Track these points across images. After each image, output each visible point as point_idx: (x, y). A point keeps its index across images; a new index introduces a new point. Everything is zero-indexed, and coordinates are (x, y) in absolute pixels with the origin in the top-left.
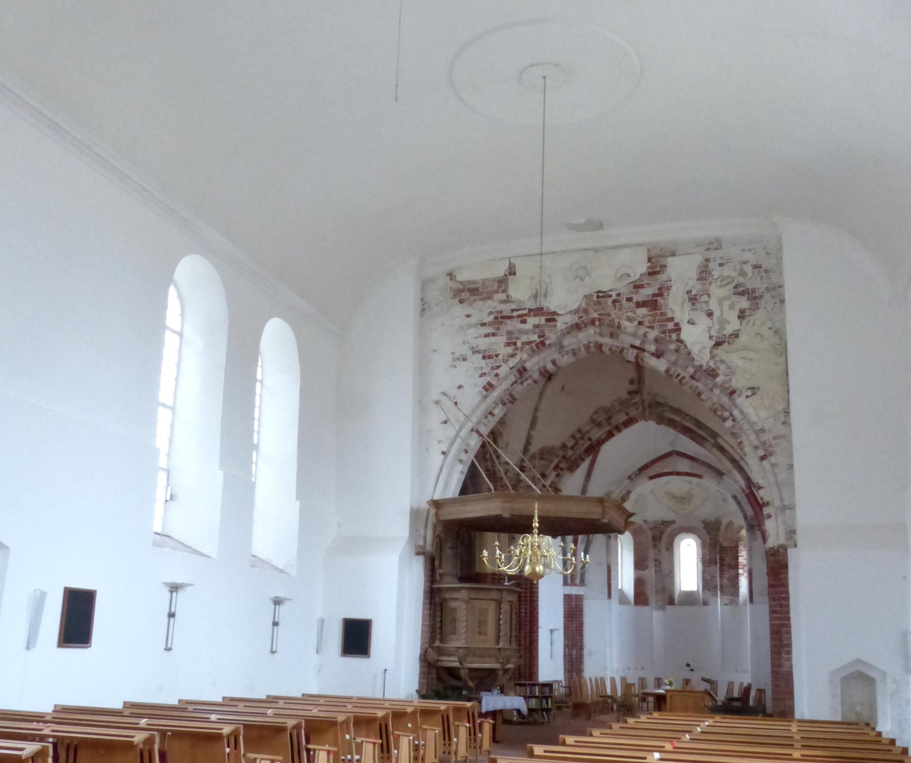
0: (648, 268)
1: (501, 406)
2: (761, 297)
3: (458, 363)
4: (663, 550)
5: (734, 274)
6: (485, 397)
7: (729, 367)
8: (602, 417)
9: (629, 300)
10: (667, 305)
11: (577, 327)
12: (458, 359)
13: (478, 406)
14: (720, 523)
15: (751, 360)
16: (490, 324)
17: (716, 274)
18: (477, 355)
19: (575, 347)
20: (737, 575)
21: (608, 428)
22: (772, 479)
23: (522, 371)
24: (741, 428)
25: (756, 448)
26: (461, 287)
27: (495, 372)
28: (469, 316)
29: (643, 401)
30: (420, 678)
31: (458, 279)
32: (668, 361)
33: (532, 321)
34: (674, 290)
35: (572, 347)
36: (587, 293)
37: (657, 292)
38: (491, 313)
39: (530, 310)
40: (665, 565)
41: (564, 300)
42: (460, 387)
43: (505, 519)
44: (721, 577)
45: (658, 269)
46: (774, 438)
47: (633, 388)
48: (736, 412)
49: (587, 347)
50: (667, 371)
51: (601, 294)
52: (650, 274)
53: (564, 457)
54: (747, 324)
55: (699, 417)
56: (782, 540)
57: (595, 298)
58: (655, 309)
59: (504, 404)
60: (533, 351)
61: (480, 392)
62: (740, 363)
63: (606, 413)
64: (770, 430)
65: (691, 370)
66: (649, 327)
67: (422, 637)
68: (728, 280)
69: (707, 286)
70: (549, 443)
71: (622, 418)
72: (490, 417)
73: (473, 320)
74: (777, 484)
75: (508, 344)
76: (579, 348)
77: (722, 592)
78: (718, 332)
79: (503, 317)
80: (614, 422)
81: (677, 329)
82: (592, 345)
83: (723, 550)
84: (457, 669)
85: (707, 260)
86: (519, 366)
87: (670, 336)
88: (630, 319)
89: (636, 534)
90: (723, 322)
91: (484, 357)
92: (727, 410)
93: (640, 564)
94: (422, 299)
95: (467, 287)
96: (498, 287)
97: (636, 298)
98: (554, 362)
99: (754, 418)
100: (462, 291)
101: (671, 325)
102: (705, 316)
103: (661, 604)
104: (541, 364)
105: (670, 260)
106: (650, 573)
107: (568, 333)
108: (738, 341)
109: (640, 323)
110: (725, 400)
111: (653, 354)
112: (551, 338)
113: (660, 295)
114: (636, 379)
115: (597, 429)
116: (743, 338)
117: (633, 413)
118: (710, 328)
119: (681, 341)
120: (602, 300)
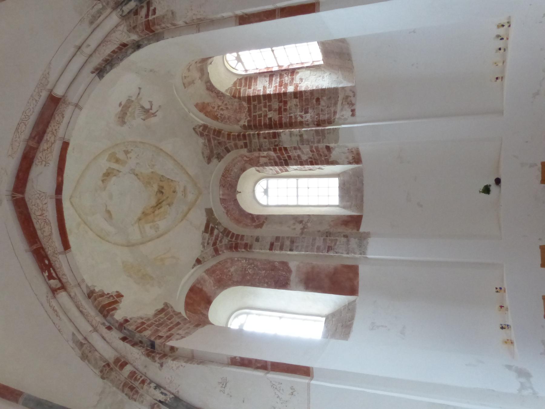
4: (258, 232)
14: (205, 127)
20: (297, 95)
40: (285, 231)
44: (301, 124)
77: (330, 122)
83: (255, 125)
89: (224, 281)
93: (279, 279)
103: (354, 242)
106: (296, 260)
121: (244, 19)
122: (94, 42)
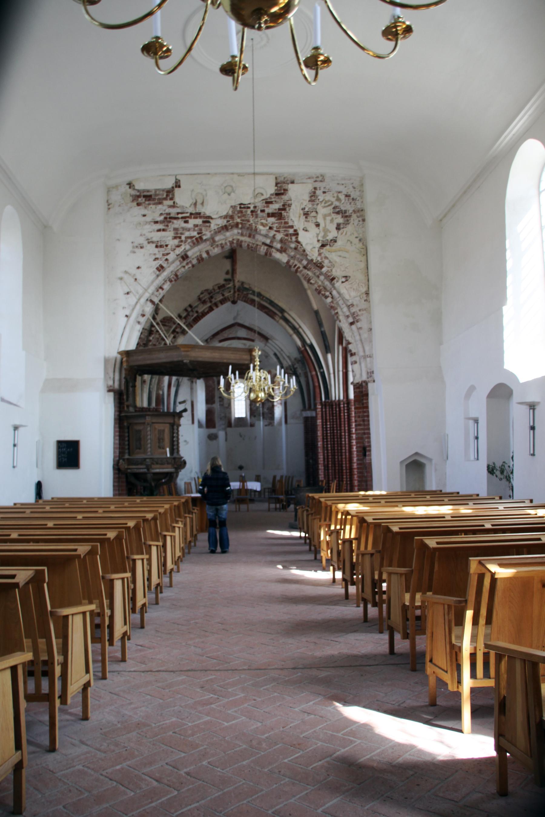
0: (276, 190)
1: (168, 283)
2: (350, 216)
3: (136, 250)
5: (333, 200)
6: (158, 276)
7: (330, 262)
8: (206, 297)
9: (263, 211)
10: (288, 217)
11: (225, 228)
12: (137, 247)
13: (153, 282)
15: (345, 257)
16: (161, 222)
17: (321, 198)
18: (151, 244)
19: (223, 242)
20: (273, 406)
21: (209, 304)
22: (358, 338)
23: (184, 257)
24: (337, 303)
25: (348, 317)
26: (138, 194)
27: (166, 257)
28: (144, 216)
29: (235, 287)
30: (114, 482)
31: (137, 187)
32: (289, 256)
33: (192, 222)
34: (293, 207)
35: (220, 242)
36: (233, 204)
37: (281, 207)
38: (161, 214)
39: (191, 214)
41: (217, 208)
42: (138, 268)
43: (185, 364)
45: (282, 192)
46: (360, 310)
47: (229, 277)
48: (334, 293)
49: (231, 243)
50: (288, 262)
51: (242, 206)
52: (277, 194)
54: (342, 234)
55: (273, 299)
56: (364, 378)
57: (238, 209)
58: (280, 219)
59: (171, 281)
60: (194, 244)
61: (154, 272)
62: (337, 259)
63: (209, 294)
64: (357, 305)
65: (305, 262)
66: (276, 231)
67: (114, 452)
68: (330, 203)
69: (315, 206)
71: (219, 297)
72: (160, 290)
73: (148, 219)
74: (361, 340)
75: (175, 238)
76: (226, 243)
77: (263, 418)
78: (324, 237)
79: (170, 218)
80: (214, 301)
81: (296, 234)
82: (235, 242)
84: (145, 474)
85: (315, 188)
86: (183, 254)
87: (291, 239)
88: (262, 224)
90: (326, 231)
91: (157, 247)
92: (328, 291)
94: (107, 201)
95: (142, 194)
96: (167, 196)
97: (267, 210)
98: (207, 252)
99: (347, 297)
100: (139, 196)
101: (291, 231)
102: (315, 226)
104: (198, 254)
105: (290, 186)
107: (219, 232)
108: (336, 244)
109: (271, 228)
110: (327, 283)
111: (277, 250)
112: (207, 235)
113: (284, 209)
114: (230, 271)
115: (202, 305)
116: (339, 243)
118: (318, 235)
119: (298, 242)
120: (244, 210)
121: (285, 404)
122: (284, 355)
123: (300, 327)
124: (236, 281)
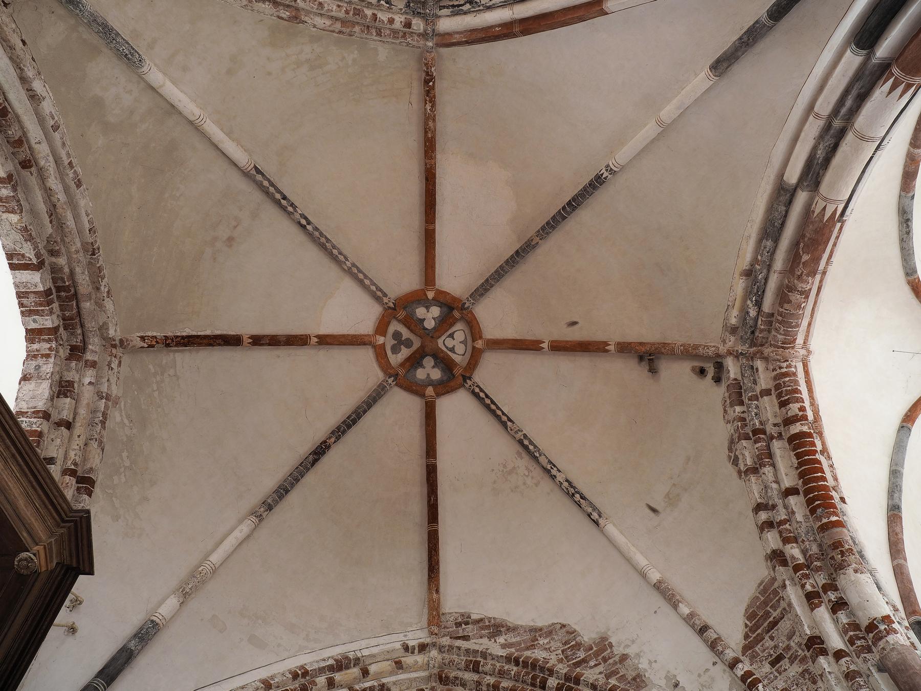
8: (748, 452)
21: (778, 447)
53: (797, 568)
70: (748, 591)
71: (769, 408)
117: (764, 380)
123: (810, 108)
124: (723, 349)
